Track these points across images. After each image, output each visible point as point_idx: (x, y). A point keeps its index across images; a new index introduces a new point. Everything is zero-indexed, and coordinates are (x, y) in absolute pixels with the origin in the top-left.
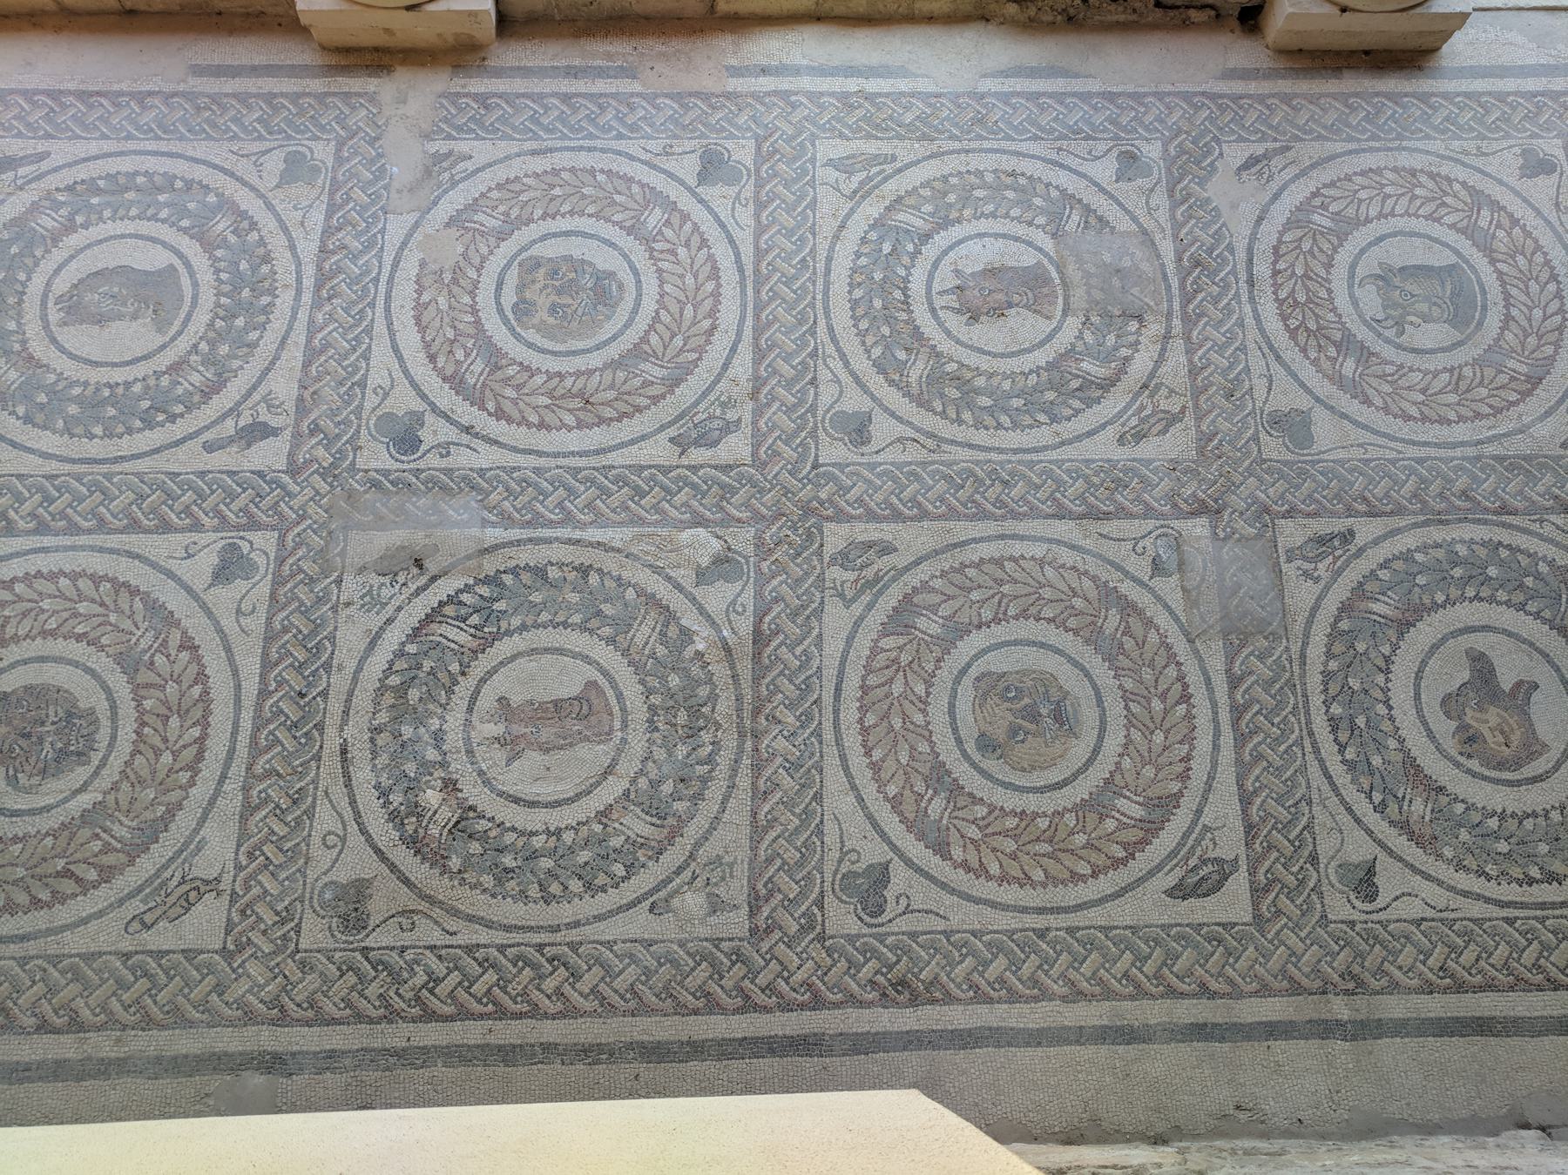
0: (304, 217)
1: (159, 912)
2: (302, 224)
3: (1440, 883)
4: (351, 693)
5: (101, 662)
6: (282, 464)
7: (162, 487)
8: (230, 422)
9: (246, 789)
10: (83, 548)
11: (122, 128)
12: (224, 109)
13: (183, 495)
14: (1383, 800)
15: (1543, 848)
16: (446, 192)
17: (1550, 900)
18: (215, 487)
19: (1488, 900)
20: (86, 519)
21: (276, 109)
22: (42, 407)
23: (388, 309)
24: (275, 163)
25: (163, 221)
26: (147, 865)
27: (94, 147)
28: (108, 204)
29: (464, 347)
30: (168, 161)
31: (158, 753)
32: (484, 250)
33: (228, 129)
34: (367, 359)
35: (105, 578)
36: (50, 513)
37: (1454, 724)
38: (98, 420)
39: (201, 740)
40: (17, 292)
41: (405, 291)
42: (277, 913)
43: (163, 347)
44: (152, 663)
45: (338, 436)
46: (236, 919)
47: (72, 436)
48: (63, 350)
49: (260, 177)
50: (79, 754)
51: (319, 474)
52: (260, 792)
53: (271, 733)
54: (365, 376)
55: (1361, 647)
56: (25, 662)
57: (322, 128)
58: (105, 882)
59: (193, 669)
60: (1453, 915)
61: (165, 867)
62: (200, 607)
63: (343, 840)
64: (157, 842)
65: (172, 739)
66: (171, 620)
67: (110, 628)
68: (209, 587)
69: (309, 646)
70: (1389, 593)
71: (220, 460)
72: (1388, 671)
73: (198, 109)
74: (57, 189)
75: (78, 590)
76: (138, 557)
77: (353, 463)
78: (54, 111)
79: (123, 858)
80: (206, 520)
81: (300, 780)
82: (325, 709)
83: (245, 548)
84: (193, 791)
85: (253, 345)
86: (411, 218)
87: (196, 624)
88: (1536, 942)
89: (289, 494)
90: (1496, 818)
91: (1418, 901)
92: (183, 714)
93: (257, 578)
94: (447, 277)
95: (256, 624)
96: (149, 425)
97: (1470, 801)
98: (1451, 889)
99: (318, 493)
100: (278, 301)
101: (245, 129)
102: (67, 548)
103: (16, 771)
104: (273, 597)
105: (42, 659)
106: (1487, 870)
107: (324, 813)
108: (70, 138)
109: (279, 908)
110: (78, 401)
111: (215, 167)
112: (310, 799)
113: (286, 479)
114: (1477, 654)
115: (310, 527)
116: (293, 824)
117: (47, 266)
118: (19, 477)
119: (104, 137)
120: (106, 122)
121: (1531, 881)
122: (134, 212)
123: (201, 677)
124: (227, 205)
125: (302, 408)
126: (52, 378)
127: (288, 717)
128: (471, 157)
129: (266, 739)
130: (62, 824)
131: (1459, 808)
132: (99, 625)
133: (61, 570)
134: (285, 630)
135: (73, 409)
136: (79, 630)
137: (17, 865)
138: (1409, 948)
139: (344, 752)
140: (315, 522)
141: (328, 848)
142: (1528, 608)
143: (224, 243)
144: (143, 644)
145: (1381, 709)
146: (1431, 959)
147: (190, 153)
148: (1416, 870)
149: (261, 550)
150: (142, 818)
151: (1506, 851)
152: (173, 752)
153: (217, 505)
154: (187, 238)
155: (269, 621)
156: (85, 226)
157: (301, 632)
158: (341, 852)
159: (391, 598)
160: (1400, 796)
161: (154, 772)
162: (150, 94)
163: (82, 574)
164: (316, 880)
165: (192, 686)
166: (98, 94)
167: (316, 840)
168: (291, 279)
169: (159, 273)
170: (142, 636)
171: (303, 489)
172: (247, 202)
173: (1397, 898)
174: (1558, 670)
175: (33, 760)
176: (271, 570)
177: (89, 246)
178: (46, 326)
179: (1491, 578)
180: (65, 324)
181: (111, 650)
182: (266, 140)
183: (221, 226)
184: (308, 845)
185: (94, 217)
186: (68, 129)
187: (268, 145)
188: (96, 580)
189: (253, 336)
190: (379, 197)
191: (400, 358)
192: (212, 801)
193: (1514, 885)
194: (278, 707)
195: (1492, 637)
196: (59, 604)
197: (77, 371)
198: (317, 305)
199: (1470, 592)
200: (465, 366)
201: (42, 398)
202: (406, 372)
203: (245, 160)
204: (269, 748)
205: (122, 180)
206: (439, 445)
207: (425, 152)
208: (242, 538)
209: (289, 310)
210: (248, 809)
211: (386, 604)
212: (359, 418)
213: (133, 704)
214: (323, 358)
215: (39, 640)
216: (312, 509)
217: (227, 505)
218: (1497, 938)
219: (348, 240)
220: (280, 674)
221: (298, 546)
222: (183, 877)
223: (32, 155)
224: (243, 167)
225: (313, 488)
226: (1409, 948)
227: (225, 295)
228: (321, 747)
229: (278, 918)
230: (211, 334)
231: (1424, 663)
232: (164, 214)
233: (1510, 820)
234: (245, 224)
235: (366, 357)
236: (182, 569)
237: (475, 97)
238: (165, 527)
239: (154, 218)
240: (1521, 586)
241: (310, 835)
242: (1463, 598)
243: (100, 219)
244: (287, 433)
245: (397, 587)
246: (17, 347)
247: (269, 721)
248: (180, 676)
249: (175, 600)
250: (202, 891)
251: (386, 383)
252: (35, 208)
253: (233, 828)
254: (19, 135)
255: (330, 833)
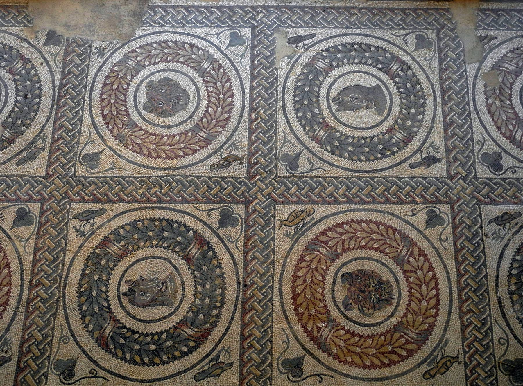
0: (430, 64)
1: (435, 370)
2: (430, 67)
4: (497, 277)
5: (388, 261)
6: (445, 175)
7: (396, 183)
8: (418, 156)
9: (461, 318)
10: (368, 210)
11: (344, 24)
12: (385, 15)
13: (406, 187)
16: (488, 53)
18: (418, 184)
20: (367, 197)
21: (407, 15)
22: (337, 147)
23: (475, 106)
24: (412, 39)
25: (370, 65)
26: (426, 349)
27: (333, 32)
28: (345, 57)
29: (512, 124)
30: (366, 38)
31: (420, 301)
32: (511, 80)
33: (388, 25)
34: (471, 128)
35: (380, 223)
36: (351, 194)
38: (362, 153)
39: (437, 295)
40: (316, 96)
41: (481, 98)
42: (486, 372)
43: (383, 121)
44: (409, 261)
45: (466, 163)
46: (469, 374)
47: (353, 160)
48: (341, 122)
49: (407, 45)
50: (387, 300)
51: (462, 179)
52: (467, 319)
53: (466, 293)
54: (472, 136)
56: (356, 259)
57: (429, 24)
58: (411, 356)
59: (426, 265)
61: (434, 351)
62: (424, 237)
63: (508, 341)
64: (428, 340)
65: (425, 295)
66: (413, 243)
67: (388, 246)
68: (426, 228)
69: (475, 255)
71: (419, 172)
73: (374, 15)
74: (322, 50)
75: (370, 228)
76: (392, 214)
77: (475, 175)
78: (313, 15)
79: (416, 347)
80: (418, 199)
81: (483, 314)
82: (487, 283)
83: (438, 212)
84: (438, 318)
85: (421, 121)
86: (477, 65)
87: (423, 244)
89: (451, 188)
92: (427, 284)
93: (445, 225)
94: (498, 92)
95: (450, 245)
96: (384, 156)
99: (463, 188)
100: (427, 102)
101: (396, 24)
102: (362, 210)
103: (362, 307)
104: (454, 235)
105: (363, 258)
107: (496, 328)
108: (322, 28)
109: (486, 370)
110: (352, 144)
111: (387, 41)
112: (489, 323)
113: (448, 181)
115: (463, 203)
116: (484, 334)
117: (326, 85)
118: (335, 178)
119: (336, 27)
120: (336, 20)
122: (356, 61)
123: (431, 268)
124: (395, 58)
125: (448, 151)
126: (338, 135)
127: (472, 287)
128: (496, 38)
129: (465, 296)
130: (387, 330)
132: (383, 244)
133: (361, 219)
134: (463, 248)
135: (350, 148)
136: (375, 246)
137: (372, 348)
139: (500, 302)
140: (465, 201)
141: (502, 345)
143: (398, 75)
144: (404, 253)
147: (374, 35)
149: (444, 213)
150: (419, 329)
152: (426, 301)
153: (421, 192)
154: (382, 73)
155: (455, 244)
156: (338, 67)
157: (469, 249)
158: (508, 347)
159: (505, 235)
161: (420, 309)
162: (352, 8)
163: (371, 221)
164: (500, 359)
165: (427, 272)
166: (331, 8)
167: (496, 341)
168: (431, 92)
169: (374, 88)
170: (402, 249)
171: (456, 186)
172: (406, 59)
175: (368, 302)
176: (450, 222)
177: (341, 76)
178: (331, 111)
180: (339, 111)
181: (391, 255)
182: (406, 29)
183: (395, 68)
184: (493, 343)
185: (340, 63)
186: (321, 24)
187: (407, 31)
188: (378, 224)
189: (420, 117)
190: (460, 55)
191: (485, 128)
192: (448, 322)
194: (467, 282)
196: (365, 235)
197: (348, 132)
198: (444, 103)
200: (514, 133)
201: (336, 143)
202: (489, 134)
203: (399, 38)
204: (466, 301)
205: (349, 47)
206: (510, 168)
207: (476, 36)
208: (435, 207)
209: (432, 106)
210: (464, 327)
211: (503, 238)
212: (474, 155)
213: (405, 279)
214: (452, 128)
215: (359, 250)
216: (462, 194)
217: (425, 192)
219: (450, 75)
220: (464, 268)
221: (460, 211)
222: (442, 355)
223: (308, 35)
224: (399, 41)
225: (461, 185)
227: (404, 98)
228: (489, 300)
229: (486, 375)
230: (402, 116)
232: (369, 62)
234: (405, 67)
235: (471, 127)
236: (412, 220)
237: (493, 11)
238: (401, 202)
239: (365, 63)
241: (493, 339)
243: (343, 64)
244: (444, 160)
245: (506, 230)
246: (321, 120)
247: (464, 288)
248: (422, 267)
249: (413, 234)
250: (452, 361)
251: (482, 139)
252: (314, 58)
253: (459, 335)
254: (301, 26)
255: (501, 338)
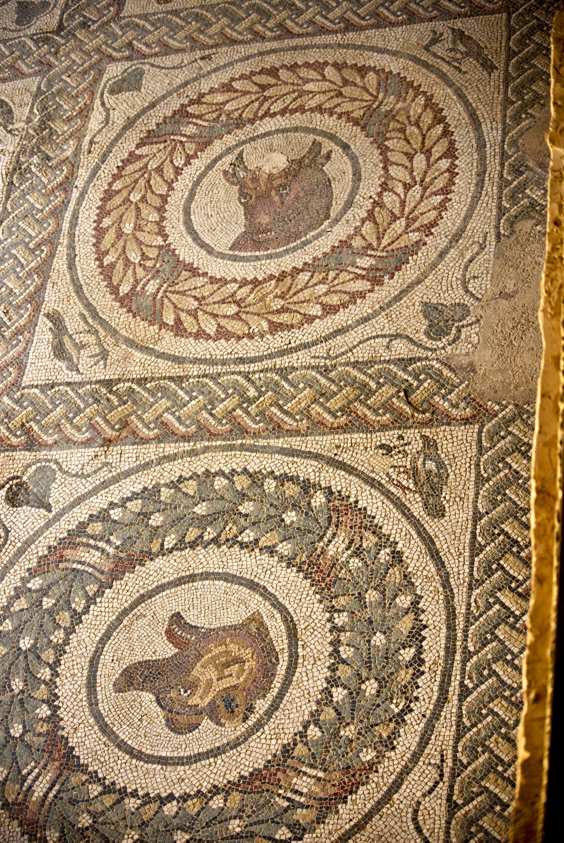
3: (406, 771)
14: (288, 826)
15: (379, 639)
17: (443, 642)
19: (436, 715)
37: (206, 723)
55: (85, 820)
60: (449, 762)
70: (25, 772)
72: (123, 792)
88: (494, 666)
90: (334, 690)
91: (426, 803)
97: (306, 718)
98: (415, 758)
106: (396, 711)
114: (123, 679)
121: (418, 660)
131: (314, 732)
138: (485, 822)
142: (79, 610)
145: (170, 809)
146: (502, 796)
148: (387, 798)
151: (376, 685)
160: (286, 804)
173: (419, 829)
174: (161, 588)
179: (34, 646)
193: (420, 682)
195: (106, 657)
199: (45, 673)
218: (484, 712)
226: (485, 822)
231: (122, 746)
233: (338, 673)
240: (51, 612)
242: (51, 684)
